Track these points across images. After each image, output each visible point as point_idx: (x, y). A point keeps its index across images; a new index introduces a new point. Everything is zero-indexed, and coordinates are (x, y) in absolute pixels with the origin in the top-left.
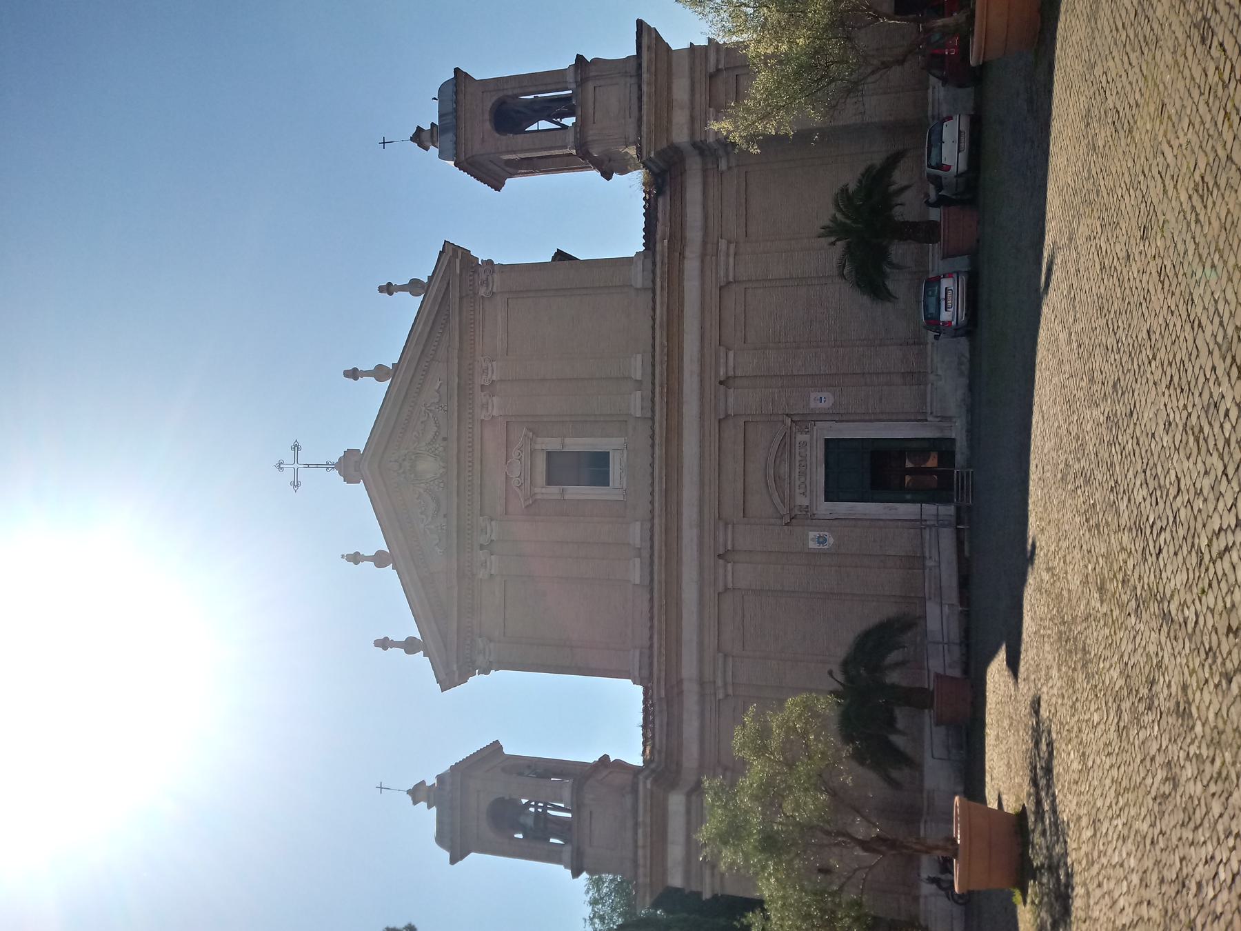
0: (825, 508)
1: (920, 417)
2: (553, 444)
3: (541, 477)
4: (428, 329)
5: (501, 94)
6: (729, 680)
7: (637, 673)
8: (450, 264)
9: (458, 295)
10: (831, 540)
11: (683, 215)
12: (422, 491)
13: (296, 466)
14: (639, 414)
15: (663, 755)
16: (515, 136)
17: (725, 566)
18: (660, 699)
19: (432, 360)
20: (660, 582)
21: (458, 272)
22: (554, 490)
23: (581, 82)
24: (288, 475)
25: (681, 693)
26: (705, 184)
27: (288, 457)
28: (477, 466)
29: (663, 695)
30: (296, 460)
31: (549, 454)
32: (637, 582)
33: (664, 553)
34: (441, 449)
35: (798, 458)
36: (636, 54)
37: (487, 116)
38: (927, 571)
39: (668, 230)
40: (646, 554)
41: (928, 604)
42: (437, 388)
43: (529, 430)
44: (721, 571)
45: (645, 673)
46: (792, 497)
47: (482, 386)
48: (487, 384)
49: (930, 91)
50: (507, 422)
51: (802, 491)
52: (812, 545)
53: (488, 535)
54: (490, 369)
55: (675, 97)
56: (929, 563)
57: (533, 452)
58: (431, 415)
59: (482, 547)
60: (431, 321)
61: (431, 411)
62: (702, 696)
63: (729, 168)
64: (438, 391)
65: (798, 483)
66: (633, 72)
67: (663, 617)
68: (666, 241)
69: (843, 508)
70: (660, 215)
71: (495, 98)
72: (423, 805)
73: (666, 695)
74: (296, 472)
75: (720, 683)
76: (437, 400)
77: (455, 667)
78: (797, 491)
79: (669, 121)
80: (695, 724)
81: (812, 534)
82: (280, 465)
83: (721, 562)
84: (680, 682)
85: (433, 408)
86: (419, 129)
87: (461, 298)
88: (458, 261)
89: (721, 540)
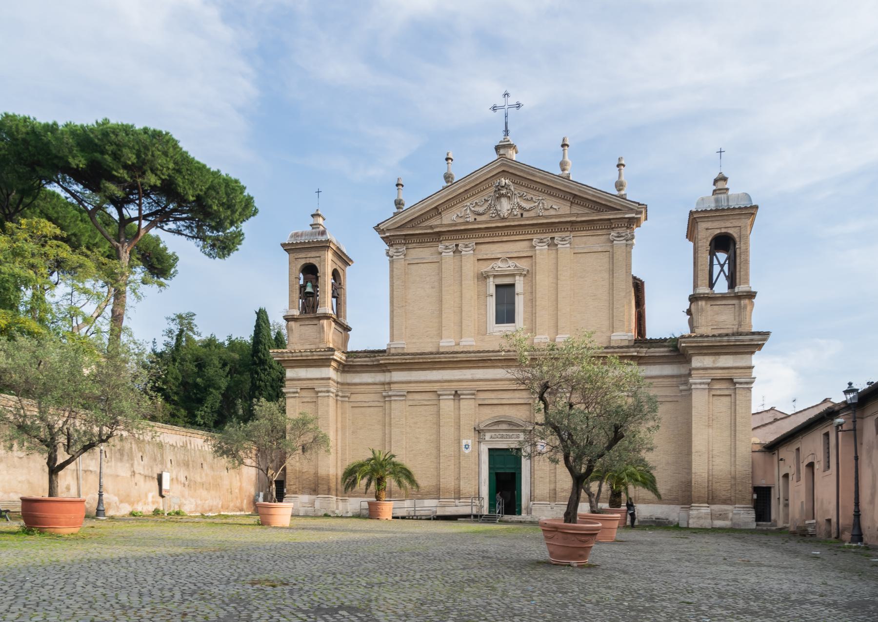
0: (484, 449)
1: (532, 498)
2: (519, 288)
3: (501, 281)
4: (590, 197)
5: (737, 240)
6: (393, 398)
7: (392, 346)
8: (631, 210)
9: (611, 217)
10: (467, 451)
11: (654, 364)
12: (489, 202)
13: (506, 107)
14: (536, 341)
15: (351, 363)
16: (708, 252)
17: (451, 395)
18: (378, 360)
19: (572, 202)
20: (439, 358)
21: (627, 216)
22: (492, 290)
23: (739, 297)
24: (500, 102)
25: (384, 371)
26: (672, 376)
27: (512, 101)
28: (505, 239)
29: (381, 362)
30: (511, 106)
31: (512, 286)
32: (441, 344)
33: (455, 359)
34: (515, 213)
35: (511, 434)
36: (753, 331)
37: (723, 231)
38: (453, 500)
39: (643, 355)
40: (457, 349)
41: (437, 501)
42: (554, 207)
43: (528, 271)
44: (449, 392)
45: (393, 351)
46: (489, 431)
47: (554, 238)
48: (556, 242)
49: (707, 505)
50: (532, 256)
51: (493, 436)
52: (464, 442)
53: (464, 249)
54: (565, 242)
55: (721, 357)
56: (457, 501)
57: (513, 275)
58: (536, 204)
59: (457, 245)
60: (594, 199)
61: (539, 204)
62: (383, 384)
63: (681, 391)
64: (551, 207)
65: (497, 434)
66: (740, 330)
67: (421, 361)
68: (635, 354)
69: (485, 458)
70: (652, 350)
71: (735, 236)
72: (312, 221)
73: (381, 364)
74: (502, 107)
75: (390, 393)
76: (546, 207)
77: (388, 234)
78: (493, 434)
79: (706, 354)
80: (370, 380)
81: (470, 442)
82: (506, 95)
83: (454, 392)
84: (389, 371)
85: (541, 205)
86: (725, 179)
87: (609, 220)
88: (633, 215)
89: (464, 392)
